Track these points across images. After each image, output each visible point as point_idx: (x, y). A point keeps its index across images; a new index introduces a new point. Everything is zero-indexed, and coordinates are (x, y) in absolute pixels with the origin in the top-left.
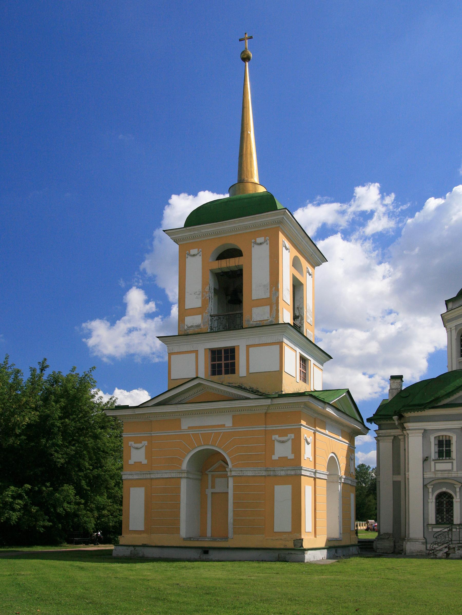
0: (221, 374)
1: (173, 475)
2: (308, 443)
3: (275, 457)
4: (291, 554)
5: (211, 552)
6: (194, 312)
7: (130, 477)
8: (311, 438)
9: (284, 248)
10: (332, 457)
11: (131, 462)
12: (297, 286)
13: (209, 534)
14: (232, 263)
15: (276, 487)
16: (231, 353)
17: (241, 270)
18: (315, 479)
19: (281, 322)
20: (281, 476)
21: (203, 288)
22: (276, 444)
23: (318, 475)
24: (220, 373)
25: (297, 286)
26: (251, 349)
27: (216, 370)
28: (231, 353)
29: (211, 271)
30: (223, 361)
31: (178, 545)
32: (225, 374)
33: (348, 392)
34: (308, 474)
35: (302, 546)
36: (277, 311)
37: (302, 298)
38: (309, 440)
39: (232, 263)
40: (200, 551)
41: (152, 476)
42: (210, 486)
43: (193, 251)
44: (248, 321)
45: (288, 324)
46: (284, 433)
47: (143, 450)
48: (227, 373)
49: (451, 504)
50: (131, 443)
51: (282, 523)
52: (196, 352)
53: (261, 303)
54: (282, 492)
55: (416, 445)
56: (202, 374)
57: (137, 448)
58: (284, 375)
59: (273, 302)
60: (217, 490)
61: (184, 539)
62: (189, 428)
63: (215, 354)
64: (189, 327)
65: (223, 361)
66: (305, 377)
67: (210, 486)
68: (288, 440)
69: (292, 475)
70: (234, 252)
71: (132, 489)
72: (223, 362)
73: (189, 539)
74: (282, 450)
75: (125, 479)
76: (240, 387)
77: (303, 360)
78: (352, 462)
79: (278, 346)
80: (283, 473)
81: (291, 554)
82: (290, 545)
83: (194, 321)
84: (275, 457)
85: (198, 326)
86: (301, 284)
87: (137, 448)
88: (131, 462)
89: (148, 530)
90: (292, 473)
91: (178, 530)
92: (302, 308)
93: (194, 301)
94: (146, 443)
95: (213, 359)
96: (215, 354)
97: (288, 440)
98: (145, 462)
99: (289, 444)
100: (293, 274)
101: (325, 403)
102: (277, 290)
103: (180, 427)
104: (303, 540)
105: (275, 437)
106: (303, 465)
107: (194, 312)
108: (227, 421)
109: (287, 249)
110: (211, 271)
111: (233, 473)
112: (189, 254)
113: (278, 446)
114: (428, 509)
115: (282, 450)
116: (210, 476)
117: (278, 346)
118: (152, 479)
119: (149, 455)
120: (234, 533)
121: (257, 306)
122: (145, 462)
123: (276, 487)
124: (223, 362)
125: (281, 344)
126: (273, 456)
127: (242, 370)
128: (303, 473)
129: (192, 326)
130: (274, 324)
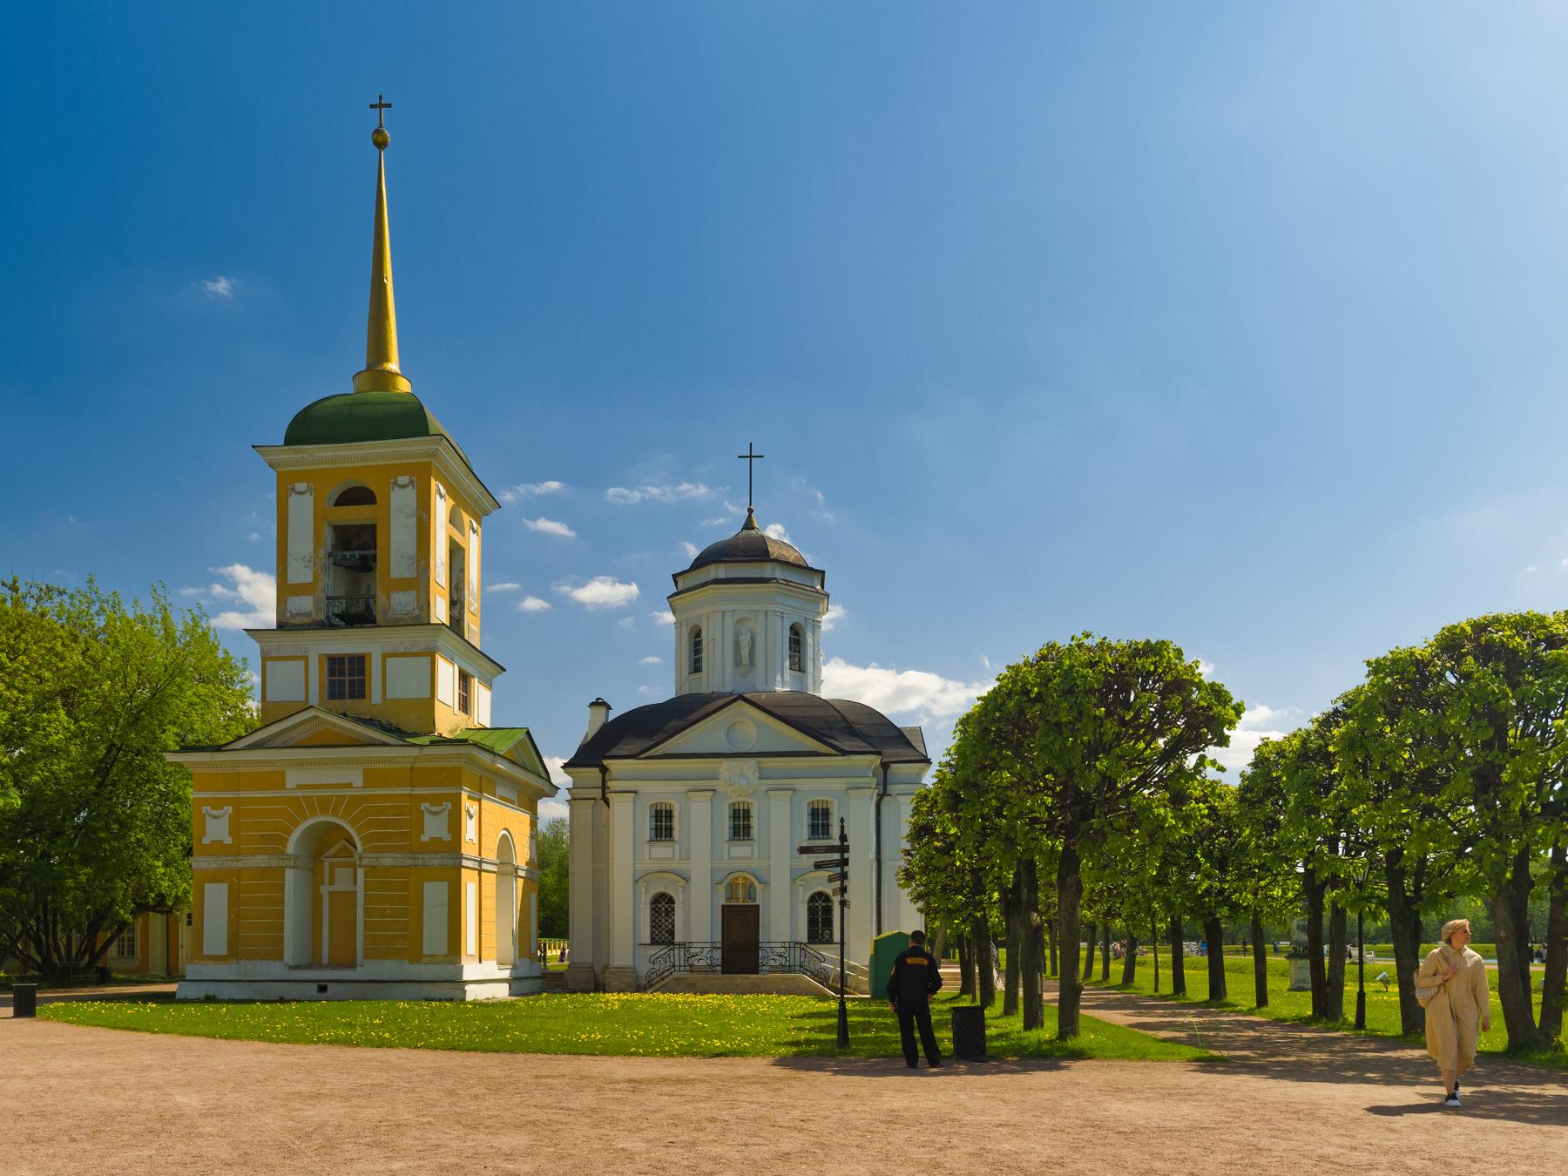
11: (206, 841)
13: (325, 960)
16: (358, 663)
18: (480, 871)
27: (335, 690)
28: (358, 663)
33: (528, 733)
42: (327, 881)
47: (226, 820)
51: (433, 940)
52: (306, 659)
54: (434, 893)
55: (626, 820)
56: (314, 699)
57: (215, 817)
60: (338, 887)
65: (346, 678)
67: (327, 881)
77: (464, 678)
87: (215, 817)
88: (206, 841)
90: (447, 860)
94: (229, 809)
95: (331, 672)
96: (335, 664)
98: (228, 841)
116: (327, 865)
119: (235, 829)
124: (347, 678)
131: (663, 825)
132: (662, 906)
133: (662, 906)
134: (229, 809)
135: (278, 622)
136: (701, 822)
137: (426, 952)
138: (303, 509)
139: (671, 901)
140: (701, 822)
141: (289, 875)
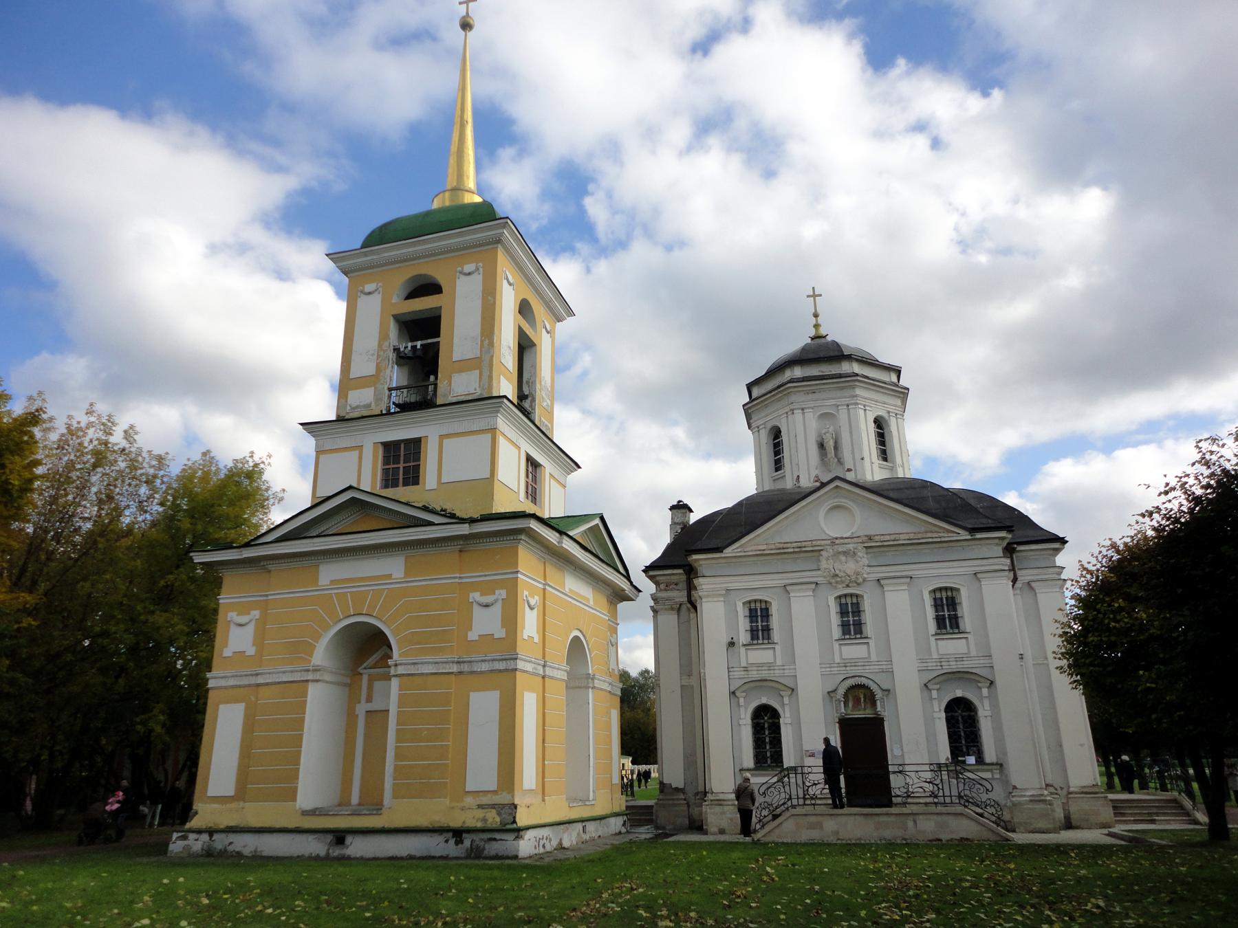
0: (397, 486)
1: (298, 677)
2: (531, 608)
3: (473, 636)
4: (495, 839)
5: (349, 839)
6: (363, 382)
7: (223, 683)
8: (537, 598)
9: (505, 282)
10: (576, 638)
11: (227, 653)
12: (525, 346)
14: (425, 303)
15: (472, 694)
17: (439, 318)
18: (543, 677)
19: (495, 394)
20: (482, 673)
21: (380, 345)
22: (477, 610)
23: (549, 672)
24: (395, 484)
25: (525, 346)
26: (446, 441)
27: (390, 480)
29: (397, 318)
30: (403, 461)
31: (291, 825)
32: (404, 485)
33: (602, 519)
34: (529, 667)
35: (514, 822)
36: (490, 377)
37: (534, 366)
38: (533, 602)
39: (425, 303)
40: (330, 837)
41: (260, 680)
43: (369, 287)
44: (445, 396)
45: (505, 397)
46: (489, 588)
47: (250, 629)
48: (406, 483)
49: (776, 729)
50: (233, 616)
51: (481, 774)
53: (466, 365)
55: (719, 616)
58: (497, 485)
59: (483, 362)
61: (305, 813)
62: (333, 582)
63: (391, 449)
64: (353, 409)
66: (533, 494)
68: (496, 601)
69: (500, 671)
70: (428, 287)
71: (221, 707)
72: (401, 465)
73: (313, 813)
74: (486, 623)
75: (213, 688)
76: (425, 509)
77: (532, 463)
78: (612, 650)
79: (489, 436)
80: (485, 667)
81: (495, 839)
82: (493, 819)
83: (363, 398)
84: (473, 636)
85: (368, 406)
86: (533, 345)
88: (227, 653)
89: (241, 793)
91: (292, 795)
92: (534, 383)
93: (364, 366)
95: (386, 460)
96: (391, 449)
97: (496, 601)
98: (251, 651)
99: (497, 609)
100: (520, 328)
101: (561, 533)
102: (491, 344)
103: (315, 581)
104: (516, 807)
105: (475, 596)
106: (521, 650)
107: (363, 382)
108: (394, 567)
109: (510, 284)
110: (395, 317)
111: (401, 670)
112: (362, 292)
113: (478, 614)
114: (740, 740)
115: (486, 623)
117: (489, 436)
118: (258, 685)
120: (396, 796)
121: (460, 371)
122: (251, 651)
123: (472, 694)
124: (401, 465)
125: (493, 431)
126: (470, 634)
127: (430, 478)
128: (521, 665)
129: (357, 407)
130: (487, 401)
131: (760, 621)
132: (766, 723)
133: (766, 723)
134: (256, 614)
135: (338, 416)
136: (806, 619)
137: (470, 787)
138: (372, 307)
139: (775, 714)
140: (806, 619)
141: (313, 691)
